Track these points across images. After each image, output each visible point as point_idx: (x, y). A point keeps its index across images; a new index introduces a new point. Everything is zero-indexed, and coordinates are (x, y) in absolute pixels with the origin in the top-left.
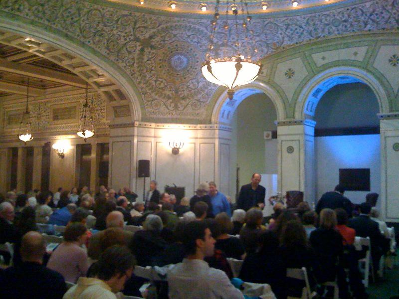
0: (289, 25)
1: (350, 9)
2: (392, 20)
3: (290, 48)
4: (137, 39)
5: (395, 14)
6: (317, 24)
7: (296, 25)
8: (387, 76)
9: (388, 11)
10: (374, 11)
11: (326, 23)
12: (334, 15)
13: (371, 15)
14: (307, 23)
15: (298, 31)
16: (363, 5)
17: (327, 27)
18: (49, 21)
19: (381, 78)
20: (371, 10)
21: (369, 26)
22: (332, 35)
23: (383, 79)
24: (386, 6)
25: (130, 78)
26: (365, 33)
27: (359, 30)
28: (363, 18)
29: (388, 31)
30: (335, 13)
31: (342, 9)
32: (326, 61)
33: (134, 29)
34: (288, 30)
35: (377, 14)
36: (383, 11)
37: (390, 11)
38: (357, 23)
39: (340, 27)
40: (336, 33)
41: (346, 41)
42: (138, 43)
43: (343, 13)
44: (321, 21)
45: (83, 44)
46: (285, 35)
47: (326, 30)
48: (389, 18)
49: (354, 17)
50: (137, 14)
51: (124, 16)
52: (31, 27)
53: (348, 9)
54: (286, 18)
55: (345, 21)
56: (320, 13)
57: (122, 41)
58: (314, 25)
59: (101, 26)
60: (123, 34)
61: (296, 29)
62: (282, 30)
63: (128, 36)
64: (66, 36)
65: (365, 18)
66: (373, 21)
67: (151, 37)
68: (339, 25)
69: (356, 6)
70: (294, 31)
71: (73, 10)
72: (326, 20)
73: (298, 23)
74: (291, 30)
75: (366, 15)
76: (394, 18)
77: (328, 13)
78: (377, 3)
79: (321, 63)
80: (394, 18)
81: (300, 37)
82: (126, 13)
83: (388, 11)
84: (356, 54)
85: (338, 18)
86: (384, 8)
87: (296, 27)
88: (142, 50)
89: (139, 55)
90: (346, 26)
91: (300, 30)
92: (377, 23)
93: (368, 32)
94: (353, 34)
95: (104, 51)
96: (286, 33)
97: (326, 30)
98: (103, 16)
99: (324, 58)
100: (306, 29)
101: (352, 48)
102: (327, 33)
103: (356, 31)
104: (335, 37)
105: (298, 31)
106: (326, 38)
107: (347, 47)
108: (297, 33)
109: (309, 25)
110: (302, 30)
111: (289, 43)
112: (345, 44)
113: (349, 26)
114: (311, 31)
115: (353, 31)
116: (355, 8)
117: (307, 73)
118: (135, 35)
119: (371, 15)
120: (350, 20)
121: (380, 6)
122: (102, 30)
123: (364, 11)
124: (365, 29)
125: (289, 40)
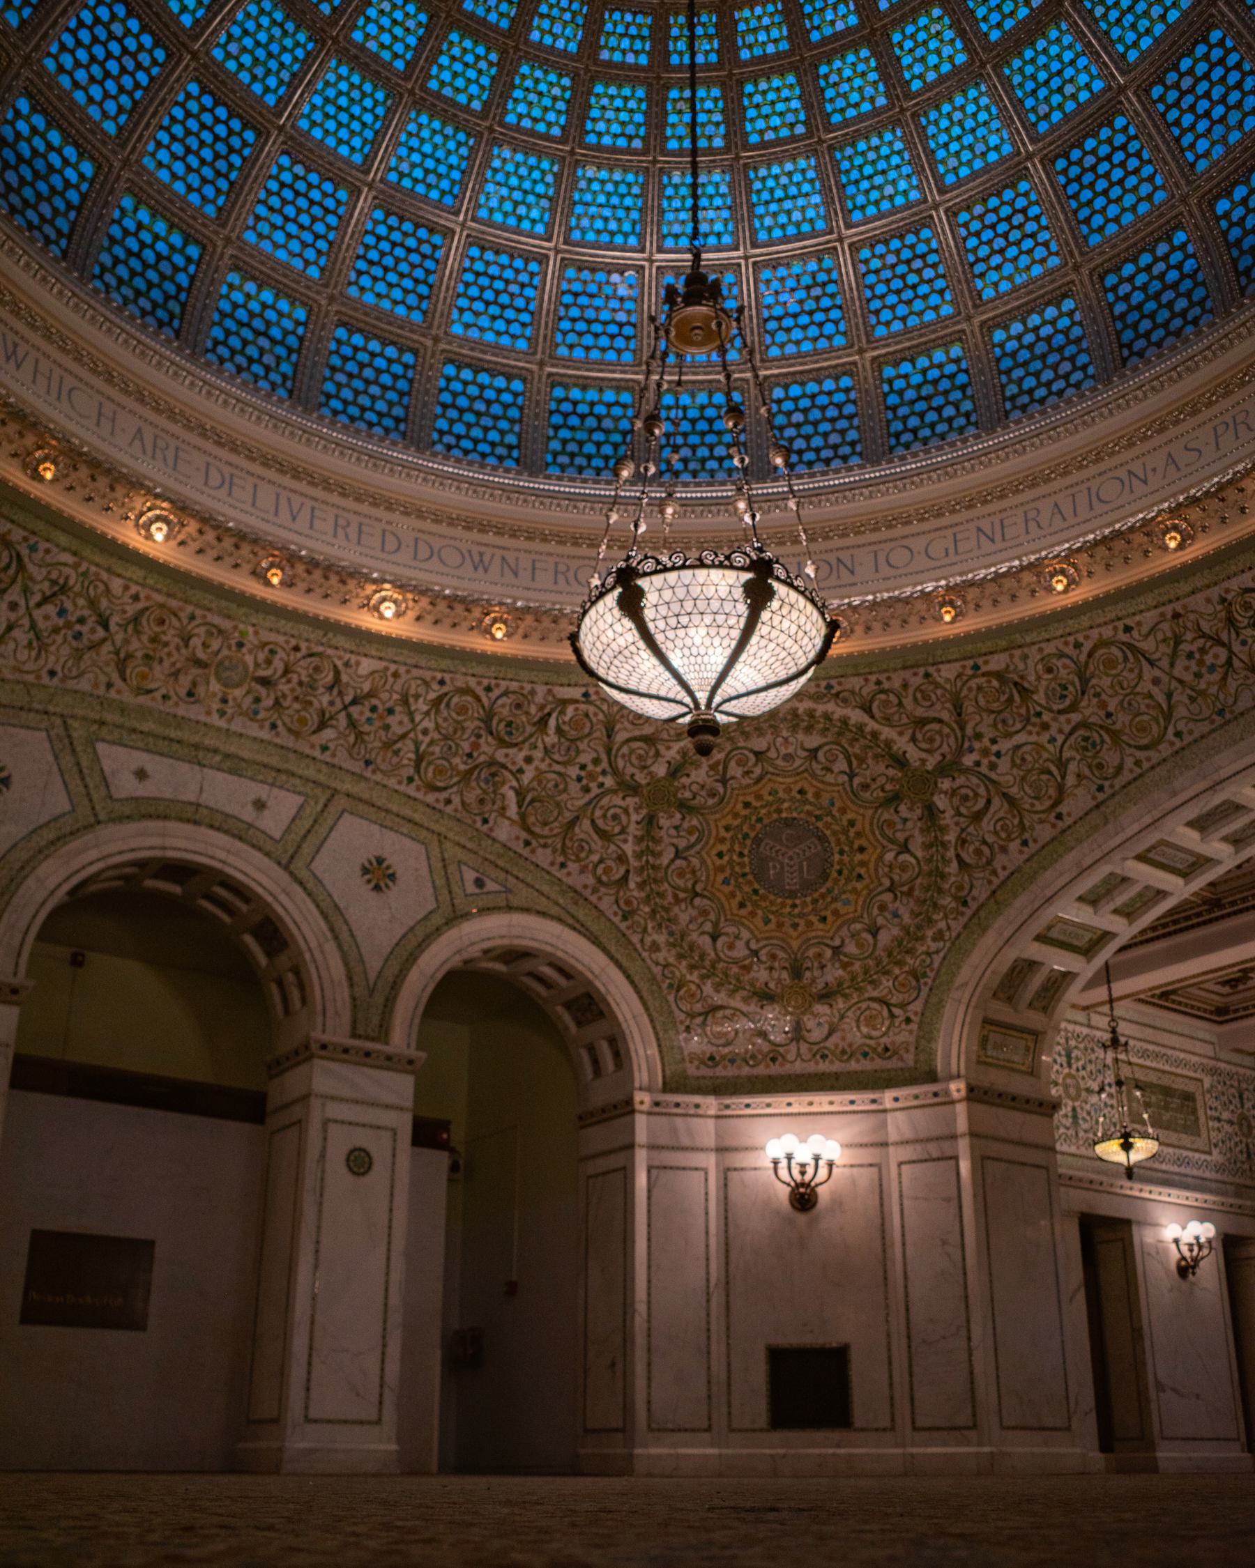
0: (64, 589)
1: (304, 652)
2: (407, 749)
3: (17, 676)
5: (425, 732)
6: (166, 644)
7: (93, 604)
8: (353, 914)
9: (411, 714)
10: (371, 694)
11: (200, 654)
12: (240, 645)
13: (355, 702)
14: (136, 620)
15: (85, 629)
16: (353, 658)
17: (196, 671)
19: (331, 913)
20: (366, 687)
21: (328, 734)
22: (195, 707)
23: (339, 924)
24: (417, 696)
26: (307, 751)
27: (290, 730)
28: (325, 699)
29: (378, 777)
30: (251, 637)
31: (281, 639)
32: (142, 790)
34: (50, 609)
35: (374, 709)
36: (398, 709)
37: (418, 718)
38: (297, 706)
39: (238, 692)
40: (216, 705)
41: (232, 749)
43: (272, 652)
44: (186, 640)
46: (26, 622)
47: (185, 681)
48: (404, 736)
49: (301, 683)
53: (296, 649)
54: (69, 558)
55: (265, 682)
56: (199, 612)
58: (154, 640)
61: (81, 621)
62: (26, 591)
65: (332, 703)
66: (352, 724)
68: (238, 685)
69: (330, 652)
70: (68, 625)
72: (205, 645)
73: (104, 603)
74: (62, 612)
75: (340, 693)
76: (417, 744)
77: (226, 625)
78: (396, 675)
79: (126, 786)
80: (417, 744)
81: (78, 654)
83: (411, 714)
84: (260, 805)
85: (249, 660)
86: (405, 701)
87: (86, 612)
90: (257, 700)
91: (93, 631)
92: (360, 735)
93: (317, 753)
94: (265, 734)
96: (37, 614)
97: (185, 681)
99: (141, 774)
100: (119, 638)
101: (252, 784)
102: (183, 692)
103: (281, 728)
104: (202, 718)
105: (85, 629)
106: (168, 707)
107: (231, 772)
108: (78, 636)
109: (138, 632)
110: (101, 633)
111: (23, 655)
112: (227, 756)
113: (269, 702)
114: (129, 656)
115: (274, 726)
116: (320, 655)
117: (67, 808)
119: (355, 702)
120: (284, 687)
121: (397, 687)
123: (344, 678)
124: (314, 738)
125: (30, 646)
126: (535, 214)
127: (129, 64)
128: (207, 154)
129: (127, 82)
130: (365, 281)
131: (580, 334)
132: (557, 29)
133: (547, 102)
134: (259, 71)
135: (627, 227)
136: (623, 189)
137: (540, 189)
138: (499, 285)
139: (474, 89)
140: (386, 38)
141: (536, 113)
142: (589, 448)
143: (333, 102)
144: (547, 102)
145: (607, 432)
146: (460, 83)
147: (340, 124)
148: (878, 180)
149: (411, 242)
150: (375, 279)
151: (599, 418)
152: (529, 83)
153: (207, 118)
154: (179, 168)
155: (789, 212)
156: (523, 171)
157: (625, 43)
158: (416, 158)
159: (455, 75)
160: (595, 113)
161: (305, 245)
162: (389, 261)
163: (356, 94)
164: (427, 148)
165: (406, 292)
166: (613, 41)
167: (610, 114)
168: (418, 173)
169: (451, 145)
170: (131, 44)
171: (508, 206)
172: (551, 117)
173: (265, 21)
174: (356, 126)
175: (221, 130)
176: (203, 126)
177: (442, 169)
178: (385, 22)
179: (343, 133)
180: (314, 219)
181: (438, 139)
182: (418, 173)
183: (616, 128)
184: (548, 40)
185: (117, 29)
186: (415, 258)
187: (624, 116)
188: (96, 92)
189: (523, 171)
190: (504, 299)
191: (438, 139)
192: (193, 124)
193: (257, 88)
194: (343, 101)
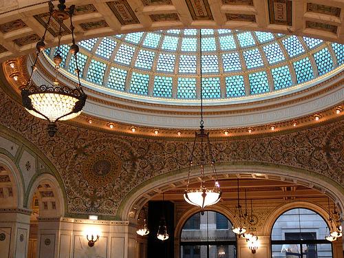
4: (319, 148)
18: (245, 159)
25: (331, 179)
33: (310, 142)
42: (322, 151)
45: (278, 166)
50: (304, 131)
51: (295, 136)
52: (234, 167)
57: (308, 154)
59: (284, 149)
60: (305, 149)
63: (310, 149)
64: (262, 164)
67: (328, 143)
71: (258, 146)
82: (295, 134)
88: (328, 155)
89: (328, 159)
95: (297, 165)
98: (281, 142)
118: (314, 146)
122: (287, 151)
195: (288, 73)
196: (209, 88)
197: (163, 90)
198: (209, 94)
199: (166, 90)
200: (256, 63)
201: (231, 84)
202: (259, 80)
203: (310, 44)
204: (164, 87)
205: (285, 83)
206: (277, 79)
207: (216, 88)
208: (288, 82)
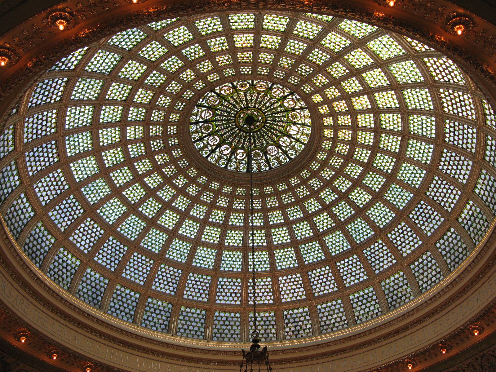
126: (407, 194)
127: (326, 276)
128: (354, 269)
129: (329, 278)
130: (404, 249)
131: (447, 201)
132: (355, 171)
133: (375, 179)
134: (341, 246)
135: (420, 172)
136: (407, 168)
137: (400, 190)
138: (423, 214)
139: (366, 197)
140: (345, 213)
141: (377, 183)
142: (479, 226)
143: (356, 232)
144: (375, 179)
145: (477, 217)
146: (363, 199)
147: (362, 233)
148: (420, 99)
149: (401, 231)
150: (405, 247)
151: (473, 215)
152: (369, 182)
153: (346, 264)
154: (353, 278)
155: (427, 126)
156: (393, 193)
157: (363, 155)
158: (379, 218)
159: (360, 200)
160: (382, 168)
161: (387, 259)
162: (402, 240)
163: (356, 226)
164: (377, 214)
165: (412, 241)
166: (362, 158)
167: (383, 164)
168: (383, 219)
169: (379, 208)
170: (322, 273)
171: (402, 201)
172: (380, 180)
173: (330, 240)
174: (364, 229)
175: (350, 263)
176: (347, 266)
177: (385, 213)
178: (341, 212)
179: (365, 233)
180: (382, 253)
181: (376, 211)
182: (383, 219)
183: (388, 164)
184: (358, 174)
185: (318, 274)
186: (405, 232)
187: (385, 161)
188: (327, 287)
189: (393, 193)
190: (428, 216)
191: (376, 211)
192: (346, 269)
193: (345, 249)
194: (357, 230)
195: (238, 323)
196: (121, 303)
197: (60, 273)
198: (118, 312)
199: (64, 276)
200: (199, 295)
201: (152, 310)
202: (192, 319)
203: (286, 296)
204: (64, 270)
205: (229, 336)
206: (218, 327)
207: (130, 307)
208: (235, 336)
